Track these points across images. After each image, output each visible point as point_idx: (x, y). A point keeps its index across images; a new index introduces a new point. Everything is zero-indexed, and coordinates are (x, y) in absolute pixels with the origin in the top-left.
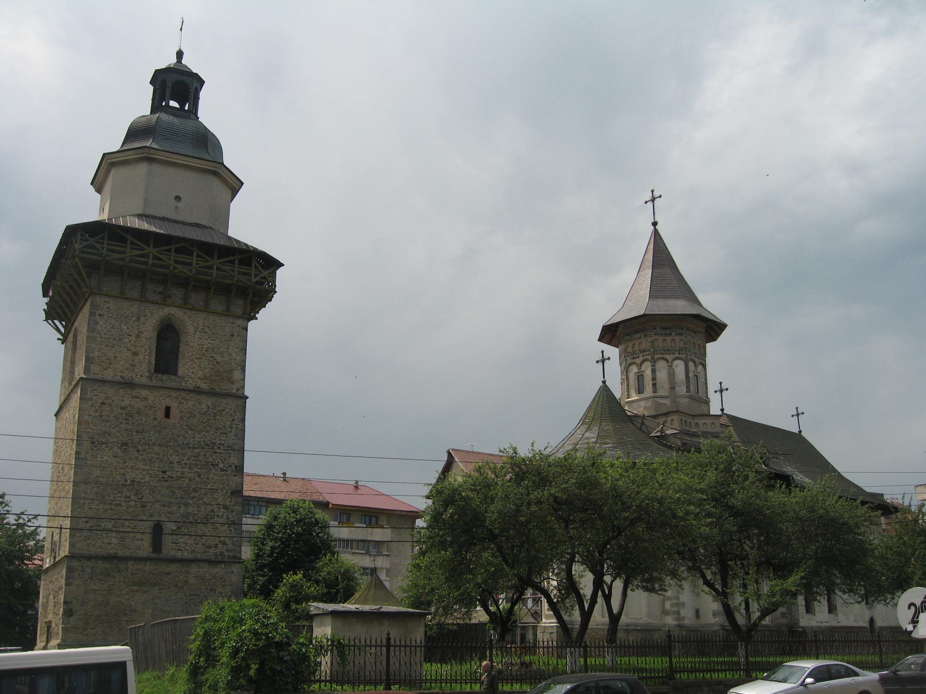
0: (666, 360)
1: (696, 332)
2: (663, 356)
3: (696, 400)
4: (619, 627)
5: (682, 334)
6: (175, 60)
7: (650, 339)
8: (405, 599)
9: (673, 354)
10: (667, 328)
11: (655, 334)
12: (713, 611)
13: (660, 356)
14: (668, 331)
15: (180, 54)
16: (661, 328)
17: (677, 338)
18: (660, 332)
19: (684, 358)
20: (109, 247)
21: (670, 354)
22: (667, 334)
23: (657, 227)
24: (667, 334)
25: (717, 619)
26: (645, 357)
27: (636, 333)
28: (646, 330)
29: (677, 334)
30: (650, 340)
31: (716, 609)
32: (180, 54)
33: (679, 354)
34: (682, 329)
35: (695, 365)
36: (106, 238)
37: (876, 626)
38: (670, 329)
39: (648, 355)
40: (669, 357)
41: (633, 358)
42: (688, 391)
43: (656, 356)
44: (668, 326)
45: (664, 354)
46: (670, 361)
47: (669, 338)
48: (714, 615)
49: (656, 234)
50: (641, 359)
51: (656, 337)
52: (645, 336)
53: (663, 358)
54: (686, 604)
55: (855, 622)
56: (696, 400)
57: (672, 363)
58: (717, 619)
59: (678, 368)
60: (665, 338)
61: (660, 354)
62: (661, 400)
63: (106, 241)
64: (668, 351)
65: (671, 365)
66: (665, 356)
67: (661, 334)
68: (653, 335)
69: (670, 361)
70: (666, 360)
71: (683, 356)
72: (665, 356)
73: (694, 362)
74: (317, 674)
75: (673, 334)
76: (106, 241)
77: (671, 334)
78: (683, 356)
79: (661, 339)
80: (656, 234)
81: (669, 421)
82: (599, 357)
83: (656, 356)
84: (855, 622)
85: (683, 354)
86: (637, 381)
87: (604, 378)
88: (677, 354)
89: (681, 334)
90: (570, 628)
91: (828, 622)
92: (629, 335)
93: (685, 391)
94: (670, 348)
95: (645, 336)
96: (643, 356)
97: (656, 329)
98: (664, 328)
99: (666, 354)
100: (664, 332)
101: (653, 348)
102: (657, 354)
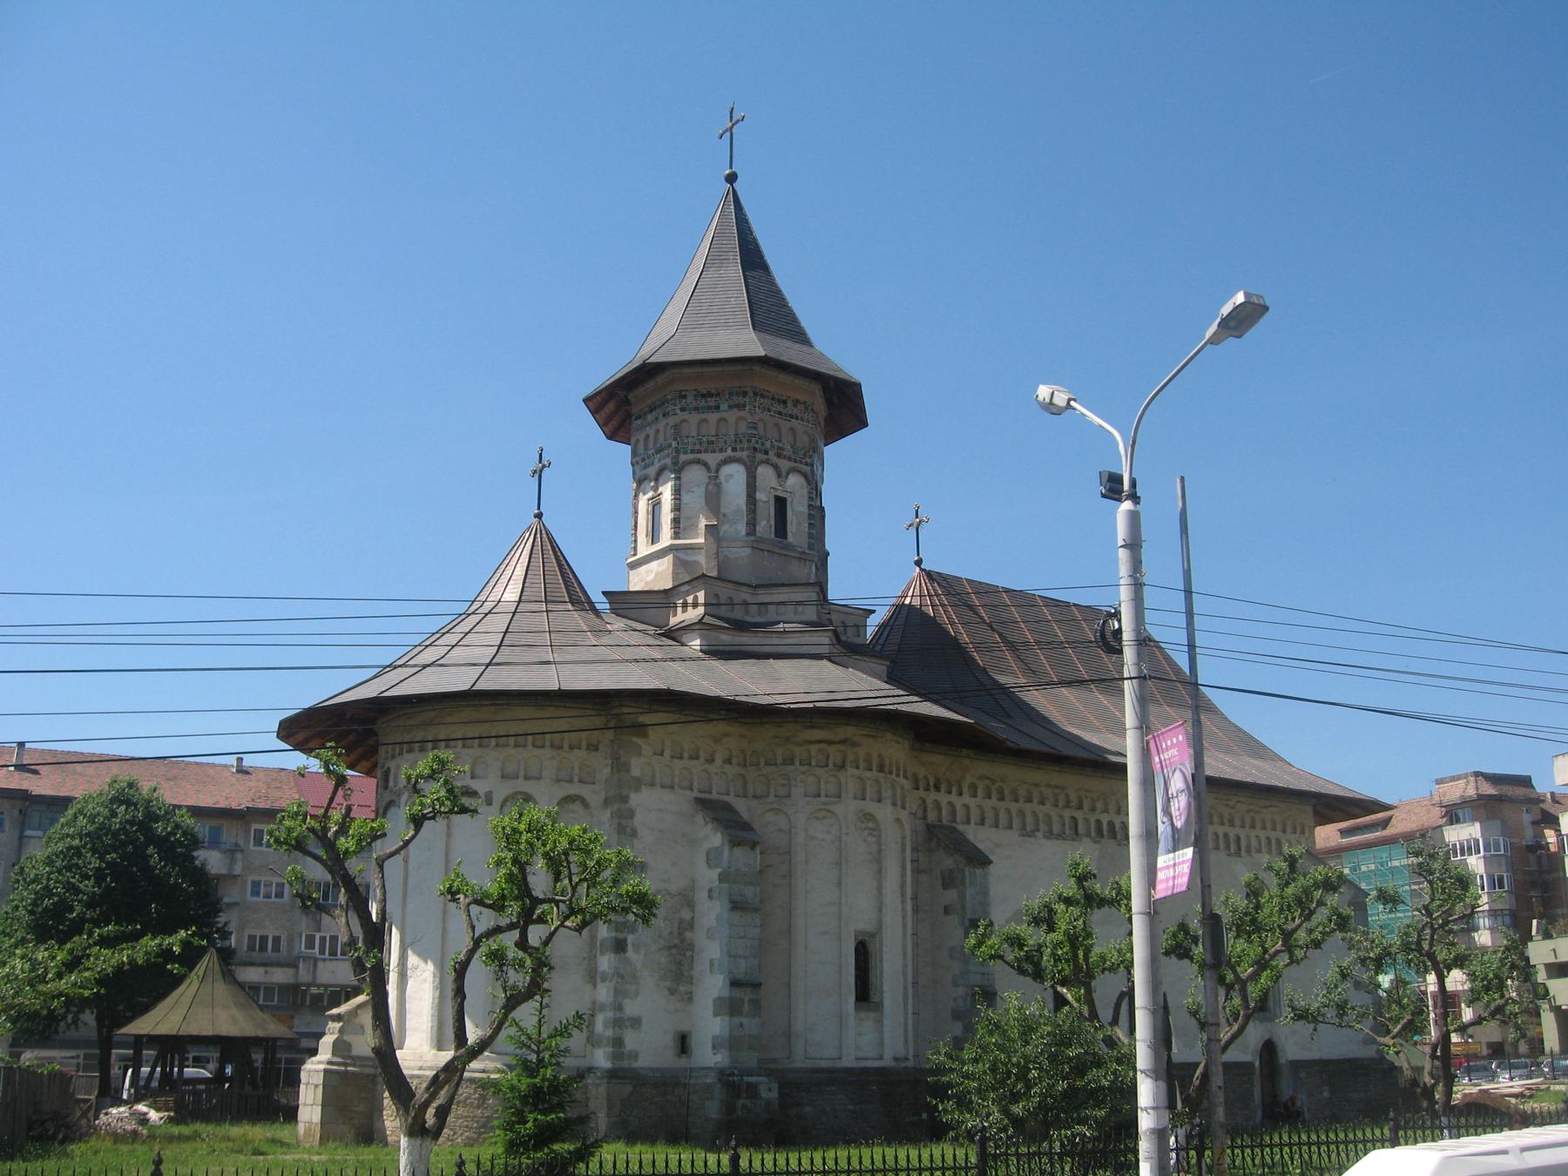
0: (706, 465)
1: (785, 402)
2: (699, 456)
4: (466, 1074)
5: (744, 406)
7: (672, 420)
9: (721, 451)
10: (710, 395)
11: (683, 410)
12: (715, 1038)
13: (690, 457)
14: (712, 402)
16: (695, 396)
17: (732, 416)
18: (694, 404)
19: (745, 458)
21: (714, 451)
22: (710, 408)
24: (710, 408)
25: (719, 1058)
26: (663, 462)
27: (651, 411)
28: (667, 401)
29: (730, 407)
30: (672, 424)
31: (718, 1033)
33: (734, 449)
34: (745, 394)
35: (779, 475)
37: (1282, 1060)
38: (718, 395)
39: (668, 455)
40: (712, 459)
41: (645, 468)
42: (752, 530)
43: (683, 458)
44: (713, 391)
45: (699, 452)
46: (713, 467)
47: (713, 417)
48: (714, 1047)
50: (657, 466)
51: (683, 416)
52: (664, 415)
53: (698, 462)
54: (644, 1021)
57: (717, 471)
58: (719, 1058)
59: (731, 481)
60: (703, 416)
61: (693, 452)
62: (687, 554)
64: (711, 446)
65: (717, 477)
66: (703, 456)
67: (696, 409)
68: (678, 412)
69: (713, 467)
70: (706, 465)
71: (744, 455)
72: (703, 456)
73: (776, 467)
75: (724, 406)
77: (717, 408)
78: (744, 455)
79: (694, 418)
82: (535, 465)
83: (683, 458)
85: (742, 450)
86: (650, 516)
87: (539, 508)
88: (729, 449)
89: (740, 407)
90: (413, 1077)
92: (640, 417)
93: (744, 532)
94: (714, 439)
95: (664, 415)
96: (660, 460)
97: (685, 397)
98: (703, 396)
99: (706, 451)
100: (703, 403)
101: (675, 439)
102: (685, 453)
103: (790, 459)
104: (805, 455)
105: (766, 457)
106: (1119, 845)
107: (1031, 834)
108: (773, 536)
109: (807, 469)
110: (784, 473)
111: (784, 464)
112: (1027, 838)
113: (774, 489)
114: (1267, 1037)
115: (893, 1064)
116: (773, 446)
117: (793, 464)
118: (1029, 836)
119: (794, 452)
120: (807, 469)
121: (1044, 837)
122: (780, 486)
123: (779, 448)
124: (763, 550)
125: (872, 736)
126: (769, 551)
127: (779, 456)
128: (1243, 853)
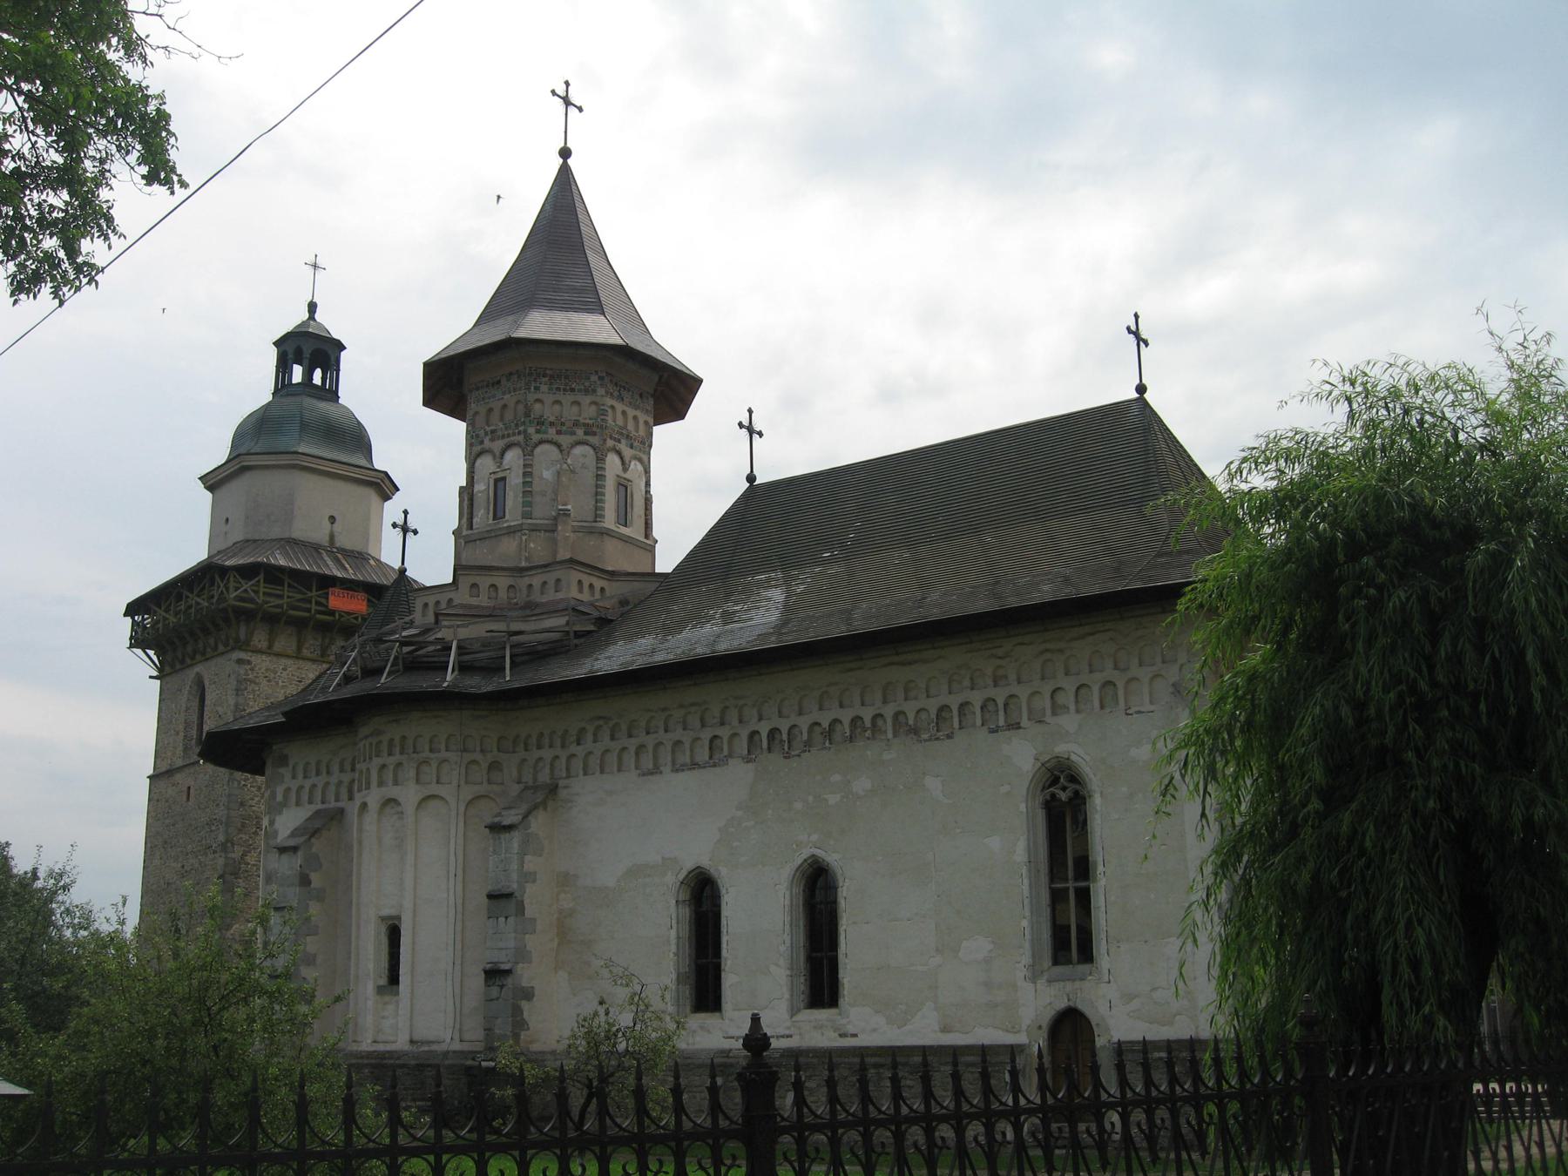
3: (485, 538)
6: (307, 316)
8: (112, 1007)
15: (312, 307)
20: (266, 590)
23: (568, 161)
32: (312, 307)
36: (262, 581)
37: (1100, 1042)
49: (565, 184)
55: (945, 1029)
56: (485, 538)
63: (262, 584)
74: (646, 1124)
76: (262, 584)
80: (565, 184)
81: (552, 583)
84: (945, 1029)
91: (791, 1036)
103: (503, 437)
104: (517, 425)
105: (482, 446)
106: (785, 757)
107: (656, 770)
108: (491, 521)
109: (520, 438)
110: (498, 454)
111: (498, 445)
112: (650, 777)
113: (494, 473)
114: (1062, 1004)
115: (407, 1047)
116: (486, 434)
117: (506, 440)
118: (652, 774)
119: (506, 429)
120: (520, 438)
121: (672, 771)
122: (499, 467)
123: (493, 432)
124: (475, 541)
125: (396, 721)
126: (480, 539)
127: (492, 440)
128: (1025, 722)
